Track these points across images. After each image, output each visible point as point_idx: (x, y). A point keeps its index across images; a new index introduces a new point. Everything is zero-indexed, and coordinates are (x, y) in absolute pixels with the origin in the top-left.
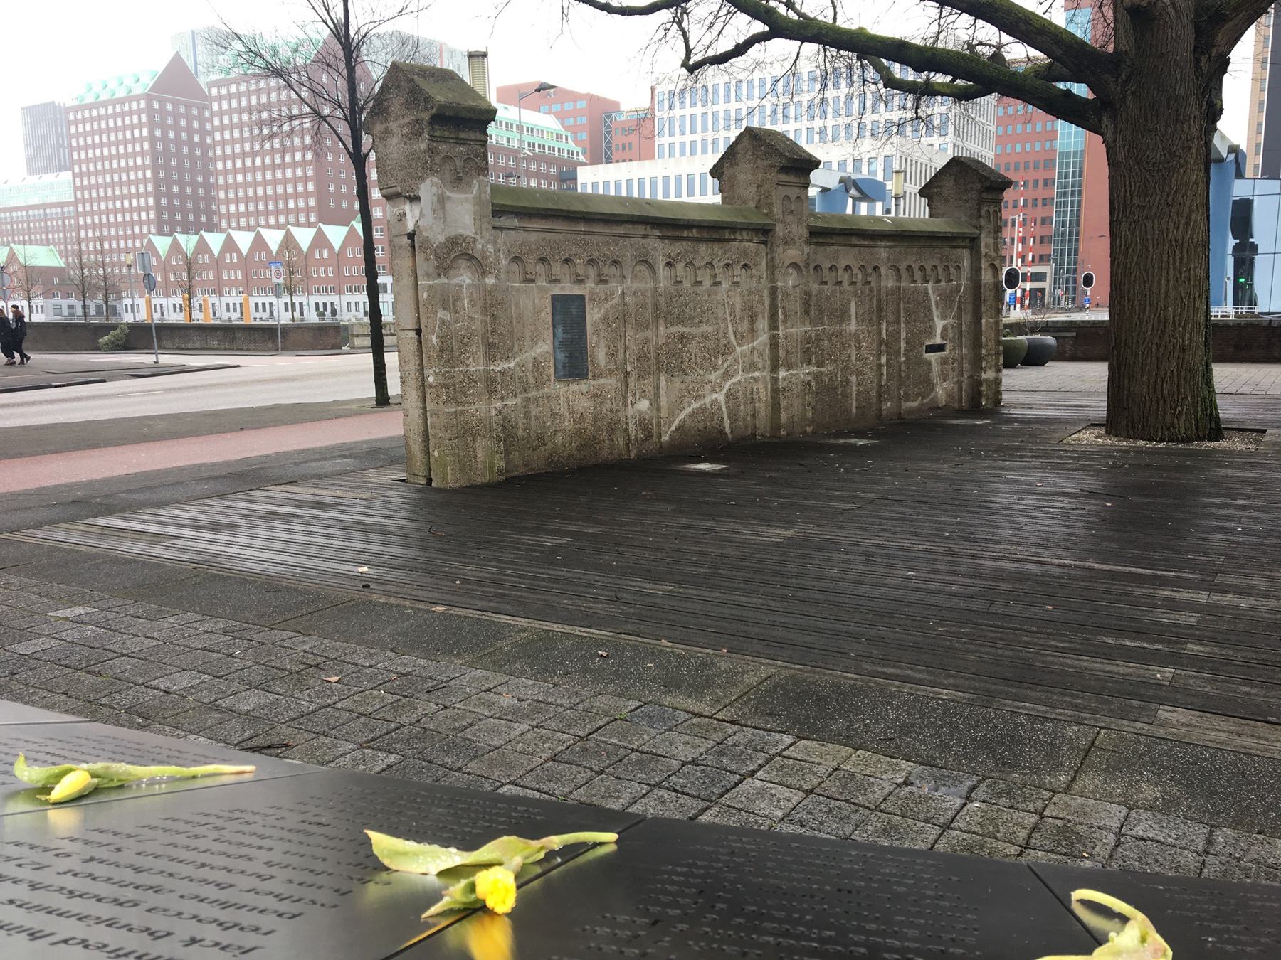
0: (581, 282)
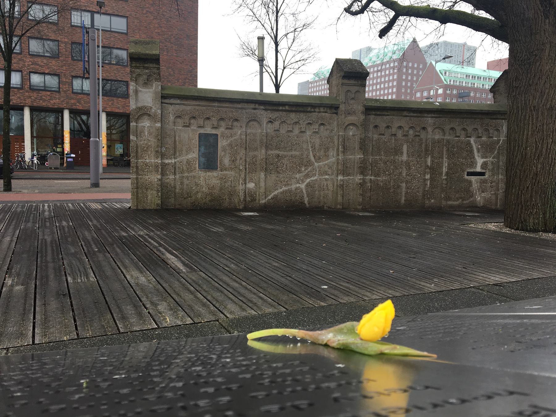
0: (216, 128)
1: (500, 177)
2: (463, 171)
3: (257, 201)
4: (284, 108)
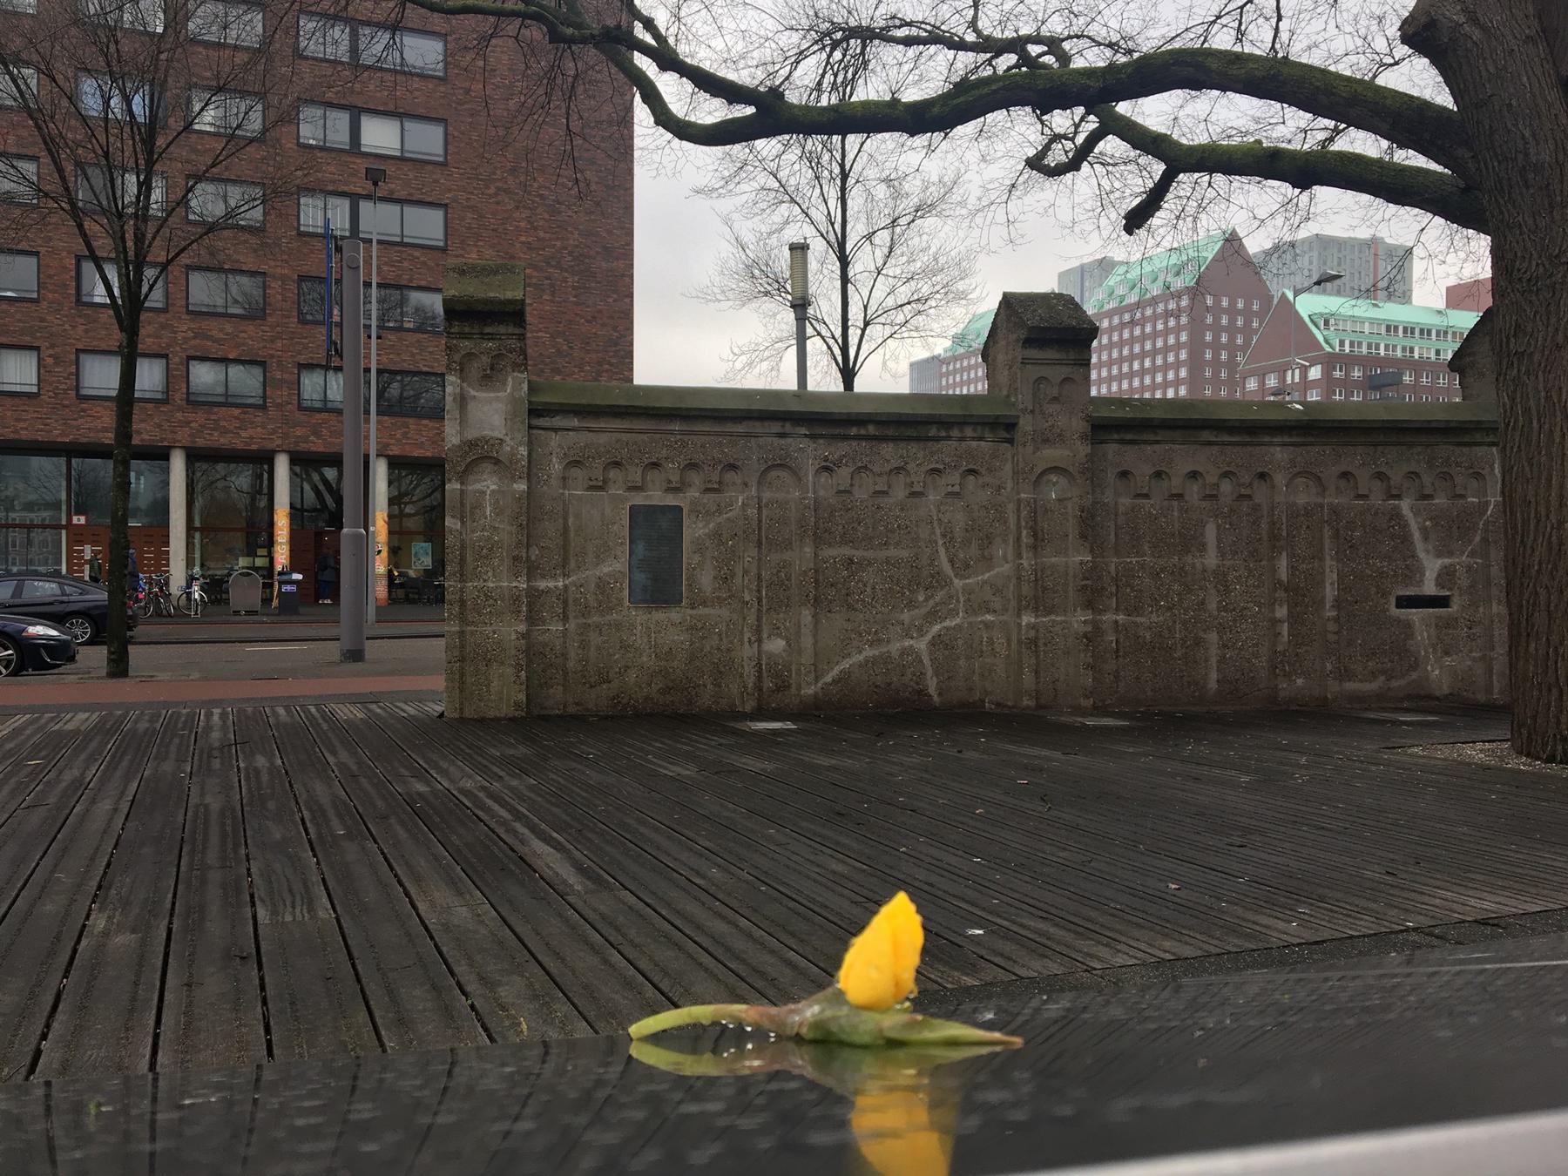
0: (676, 490)
1: (1495, 609)
2: (1385, 595)
3: (793, 690)
4: (863, 432)
